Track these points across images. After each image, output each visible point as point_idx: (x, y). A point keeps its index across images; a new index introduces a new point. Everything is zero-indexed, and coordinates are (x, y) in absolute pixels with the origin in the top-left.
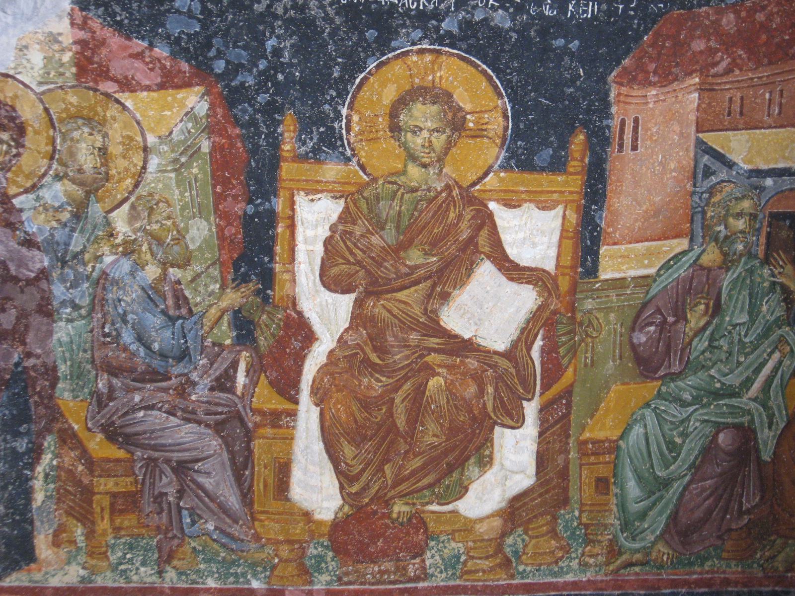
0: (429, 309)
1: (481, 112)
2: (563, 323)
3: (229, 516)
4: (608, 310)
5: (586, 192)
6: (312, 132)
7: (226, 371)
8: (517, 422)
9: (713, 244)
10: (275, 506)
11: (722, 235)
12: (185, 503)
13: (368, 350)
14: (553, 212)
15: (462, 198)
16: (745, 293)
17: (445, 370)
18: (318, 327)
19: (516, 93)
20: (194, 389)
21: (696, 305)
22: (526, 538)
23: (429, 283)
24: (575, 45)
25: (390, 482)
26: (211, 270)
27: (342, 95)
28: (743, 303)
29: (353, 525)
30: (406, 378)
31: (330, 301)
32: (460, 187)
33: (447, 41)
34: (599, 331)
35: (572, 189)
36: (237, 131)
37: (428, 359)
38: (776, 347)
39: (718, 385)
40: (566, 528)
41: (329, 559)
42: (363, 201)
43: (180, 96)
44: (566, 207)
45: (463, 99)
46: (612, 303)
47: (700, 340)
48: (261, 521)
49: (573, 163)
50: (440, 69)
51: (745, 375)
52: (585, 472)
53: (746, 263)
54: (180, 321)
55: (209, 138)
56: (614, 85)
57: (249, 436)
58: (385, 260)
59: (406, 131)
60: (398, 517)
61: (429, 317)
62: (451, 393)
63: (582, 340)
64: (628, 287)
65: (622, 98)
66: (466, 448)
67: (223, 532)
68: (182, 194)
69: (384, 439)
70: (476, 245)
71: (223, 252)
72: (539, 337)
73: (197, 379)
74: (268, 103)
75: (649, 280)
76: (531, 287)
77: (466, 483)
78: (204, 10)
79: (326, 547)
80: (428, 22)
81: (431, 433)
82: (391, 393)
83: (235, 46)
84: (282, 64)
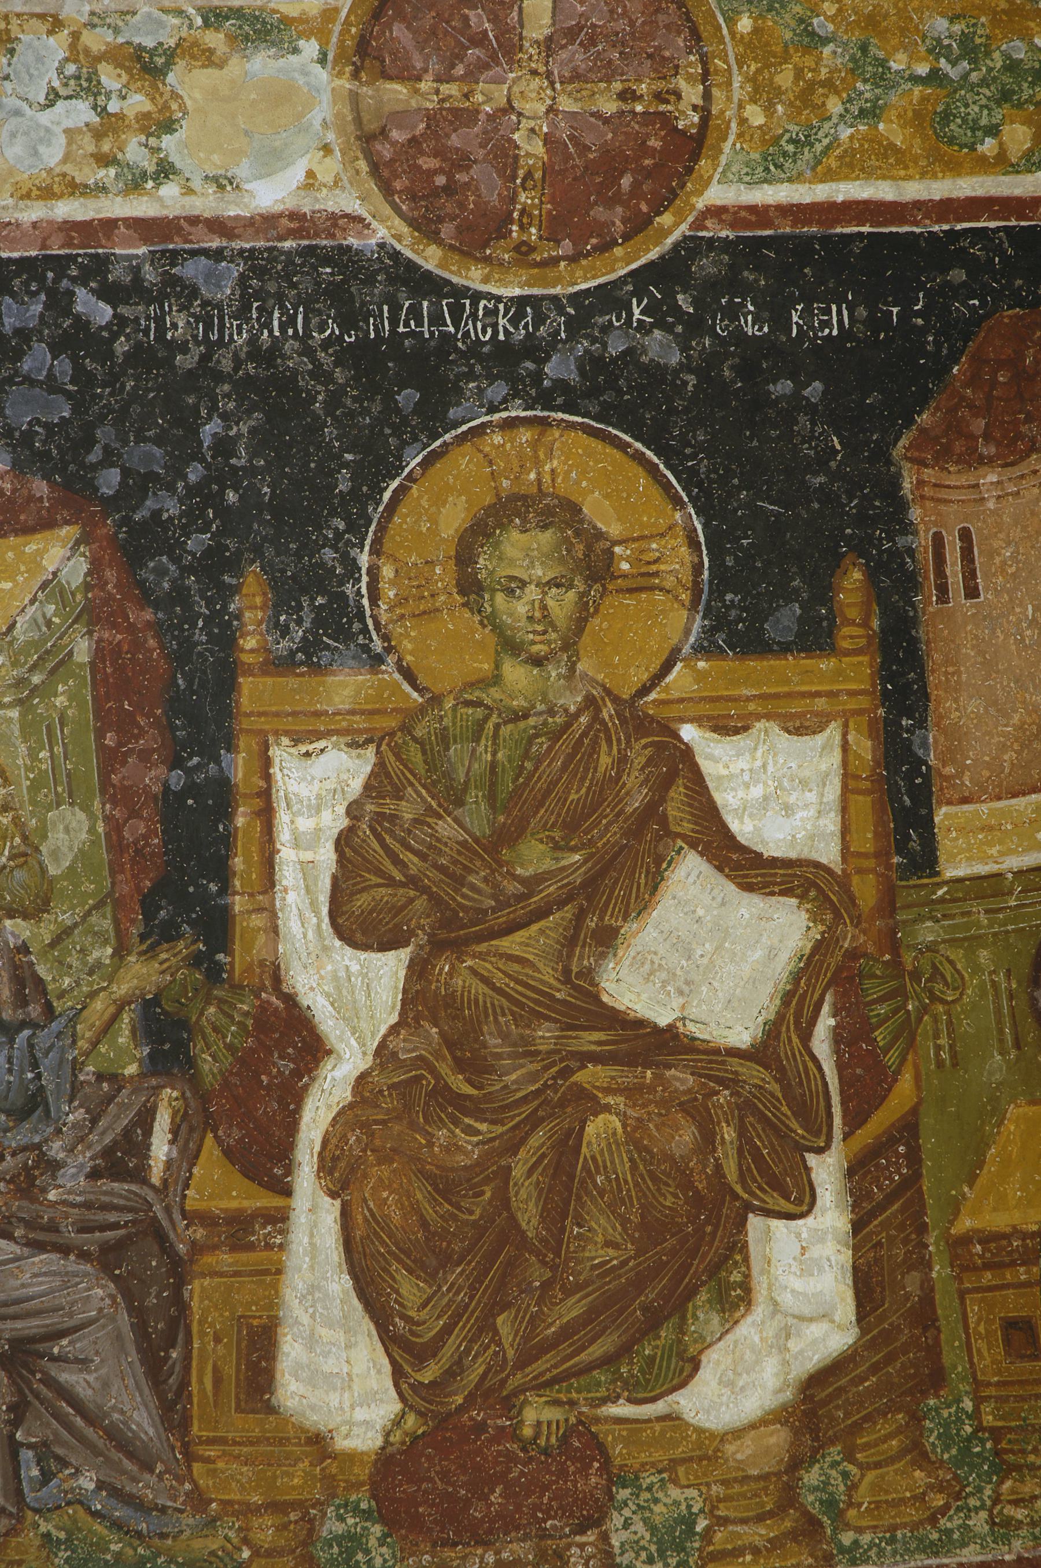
0: (575, 969)
1: (642, 538)
2: (875, 976)
3: (131, 1456)
4: (972, 943)
5: (885, 692)
6: (300, 608)
7: (127, 1132)
8: (799, 1202)
10: (240, 1424)
12: (28, 1434)
13: (444, 1069)
14: (820, 739)
15: (623, 721)
17: (621, 1099)
18: (328, 1022)
19: (709, 496)
20: (54, 1177)
22: (852, 1469)
23: (569, 911)
24: (814, 390)
25: (511, 1353)
26: (93, 919)
27: (357, 526)
29: (429, 1458)
30: (534, 1122)
31: (355, 968)
32: (616, 700)
33: (559, 401)
34: (960, 987)
35: (854, 687)
36: (148, 615)
37: (579, 1077)
40: (946, 1438)
41: (373, 1542)
42: (414, 747)
43: (31, 548)
44: (846, 725)
45: (601, 513)
46: (979, 927)
48: (208, 1460)
49: (846, 631)
50: (550, 455)
52: (973, 1310)
54: (26, 1033)
55: (90, 633)
56: (906, 465)
57: (179, 1271)
58: (469, 871)
59: (494, 591)
60: (537, 1436)
61: (576, 988)
62: (640, 1148)
63: (924, 1009)
64: (1010, 893)
65: (927, 491)
66: (686, 1267)
67: (116, 1493)
68: (33, 754)
69: (491, 1257)
70: (664, 821)
71: (120, 877)
72: (826, 1008)
73: (62, 1155)
74: (208, 552)
76: (794, 901)
77: (692, 1351)
78: (80, 374)
79: (366, 1515)
80: (517, 364)
81: (600, 1239)
82: (501, 1155)
83: (140, 439)
84: (235, 469)
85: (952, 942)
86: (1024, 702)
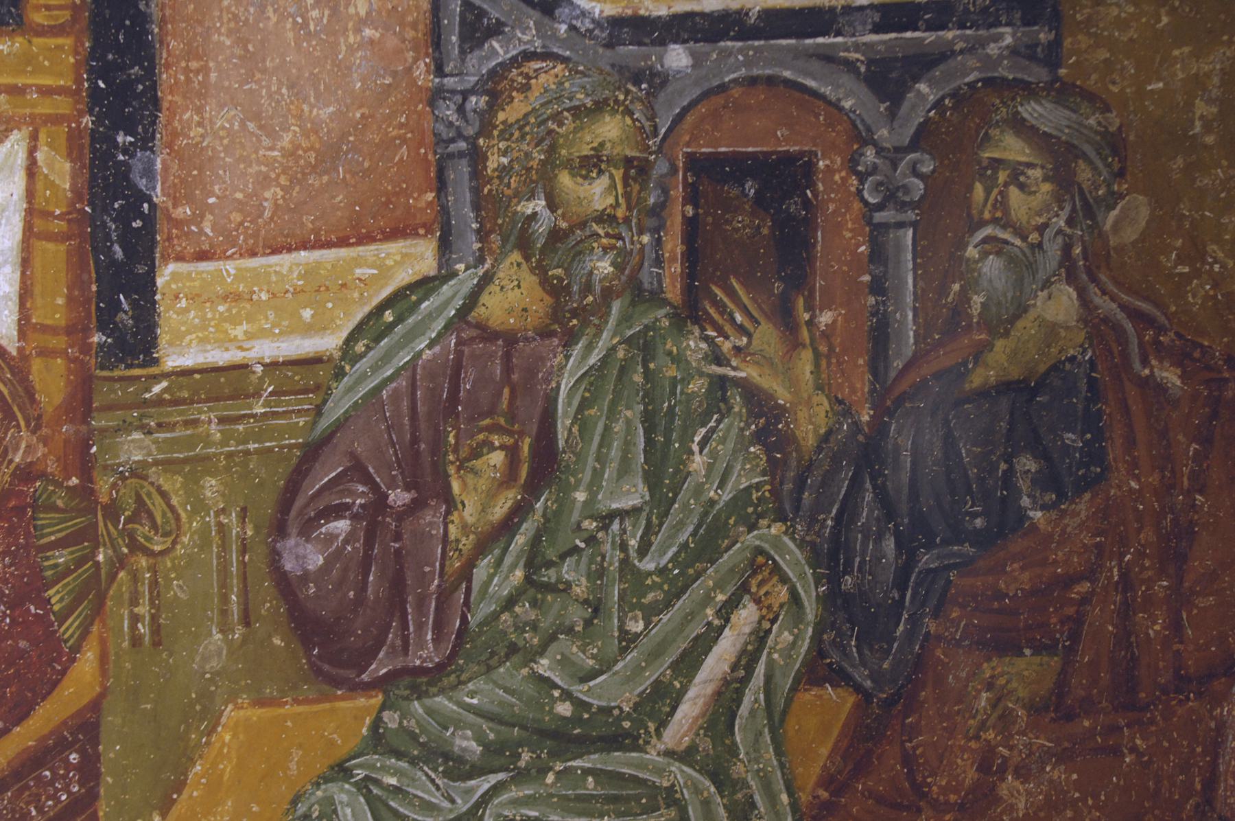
2: (54, 508)
4: (199, 466)
5: (94, 91)
9: (516, 256)
11: (542, 228)
16: (632, 413)
21: (476, 454)
28: (627, 445)
34: (173, 532)
35: (48, 81)
38: (744, 588)
39: (564, 709)
44: (34, 137)
46: (208, 444)
47: (499, 563)
51: (650, 676)
53: (625, 319)
63: (120, 562)
64: (257, 394)
75: (322, 372)
85: (168, 465)
86: (300, 117)
